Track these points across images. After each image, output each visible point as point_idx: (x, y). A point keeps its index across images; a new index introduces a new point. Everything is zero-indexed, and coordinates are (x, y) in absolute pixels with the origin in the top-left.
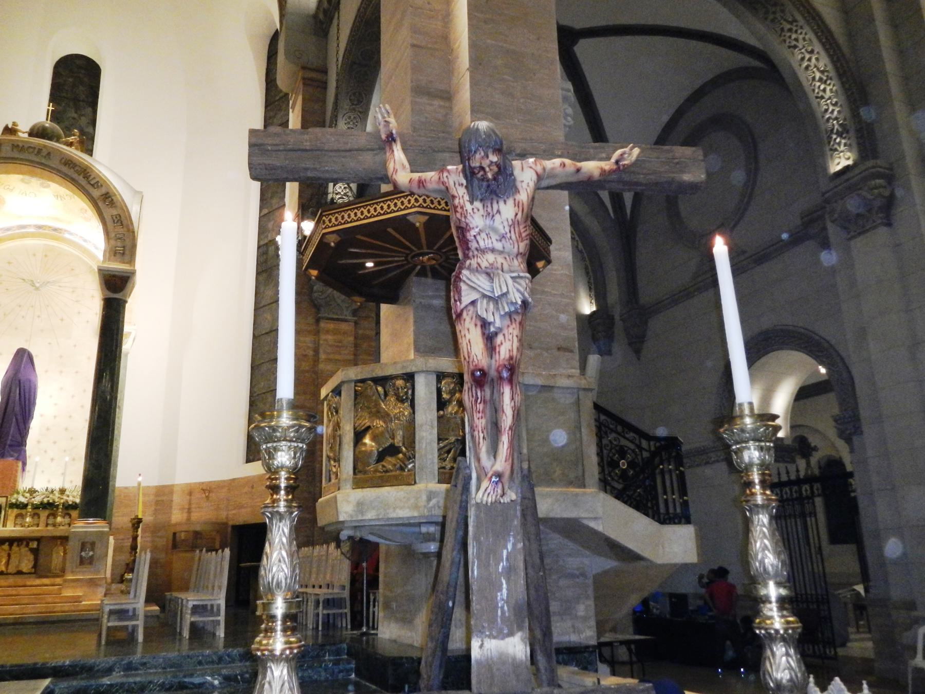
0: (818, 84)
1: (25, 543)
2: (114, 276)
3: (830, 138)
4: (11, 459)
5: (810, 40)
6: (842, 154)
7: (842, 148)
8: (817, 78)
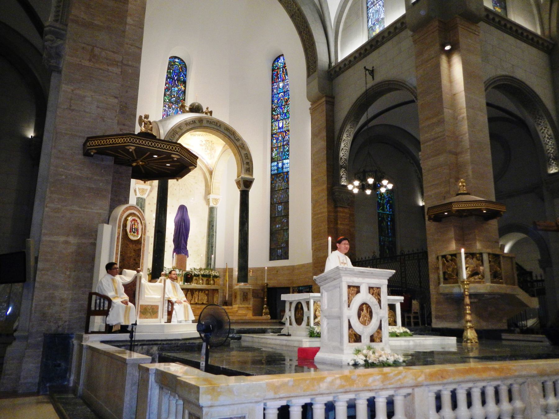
0: (546, 139)
1: (203, 291)
3: (549, 161)
4: (183, 254)
5: (546, 123)
6: (553, 167)
7: (554, 165)
8: (546, 137)
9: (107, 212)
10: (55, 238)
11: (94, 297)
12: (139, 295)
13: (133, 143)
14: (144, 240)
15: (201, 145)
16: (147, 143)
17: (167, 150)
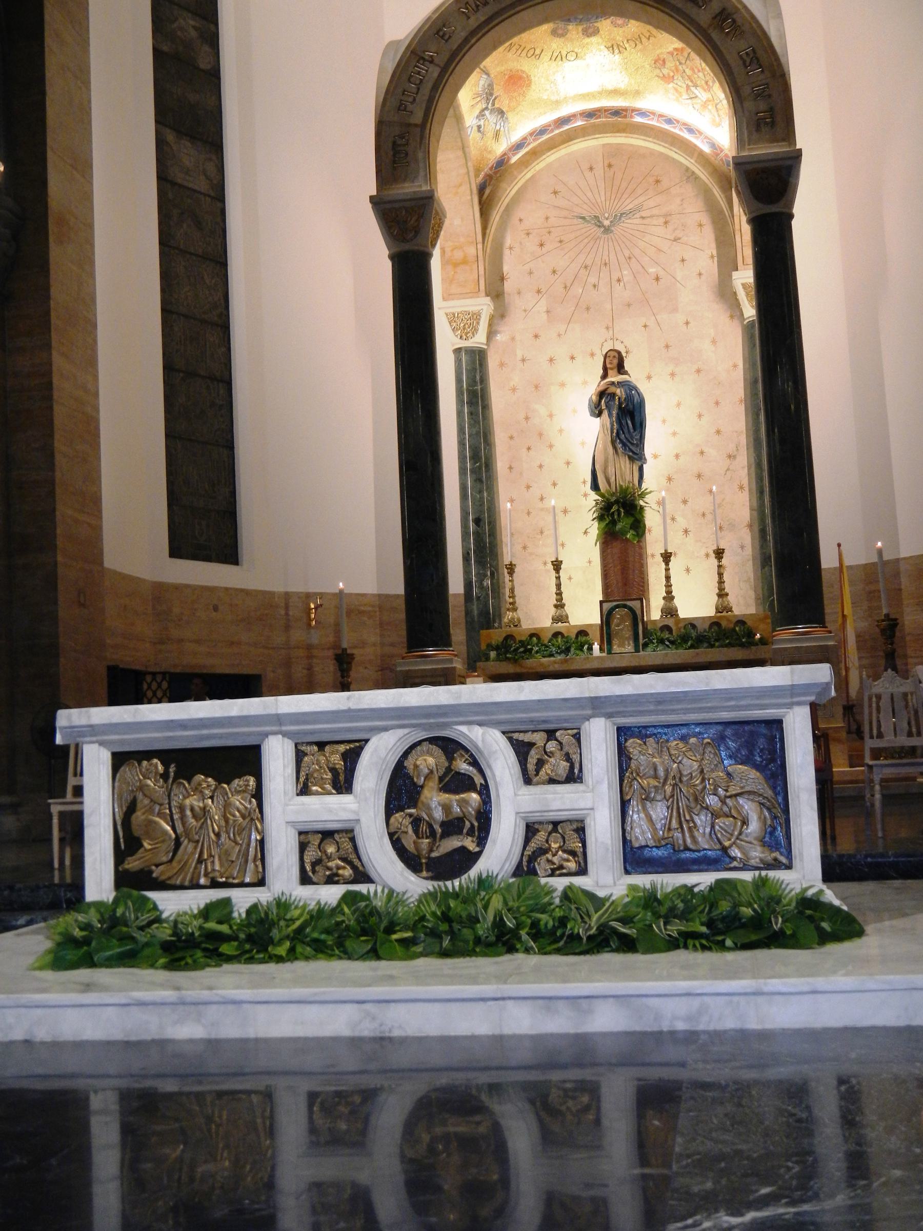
2: (764, 171)
15: (667, 79)
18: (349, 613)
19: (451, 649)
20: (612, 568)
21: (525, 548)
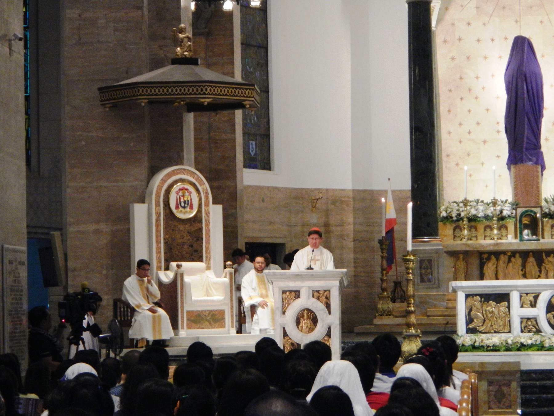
4: (530, 163)
9: (144, 183)
10: (83, 228)
11: (118, 303)
12: (182, 298)
13: (144, 95)
14: (208, 214)
16: (161, 90)
17: (191, 94)
18: (334, 202)
19: (438, 237)
20: (519, 184)
21: (457, 164)
